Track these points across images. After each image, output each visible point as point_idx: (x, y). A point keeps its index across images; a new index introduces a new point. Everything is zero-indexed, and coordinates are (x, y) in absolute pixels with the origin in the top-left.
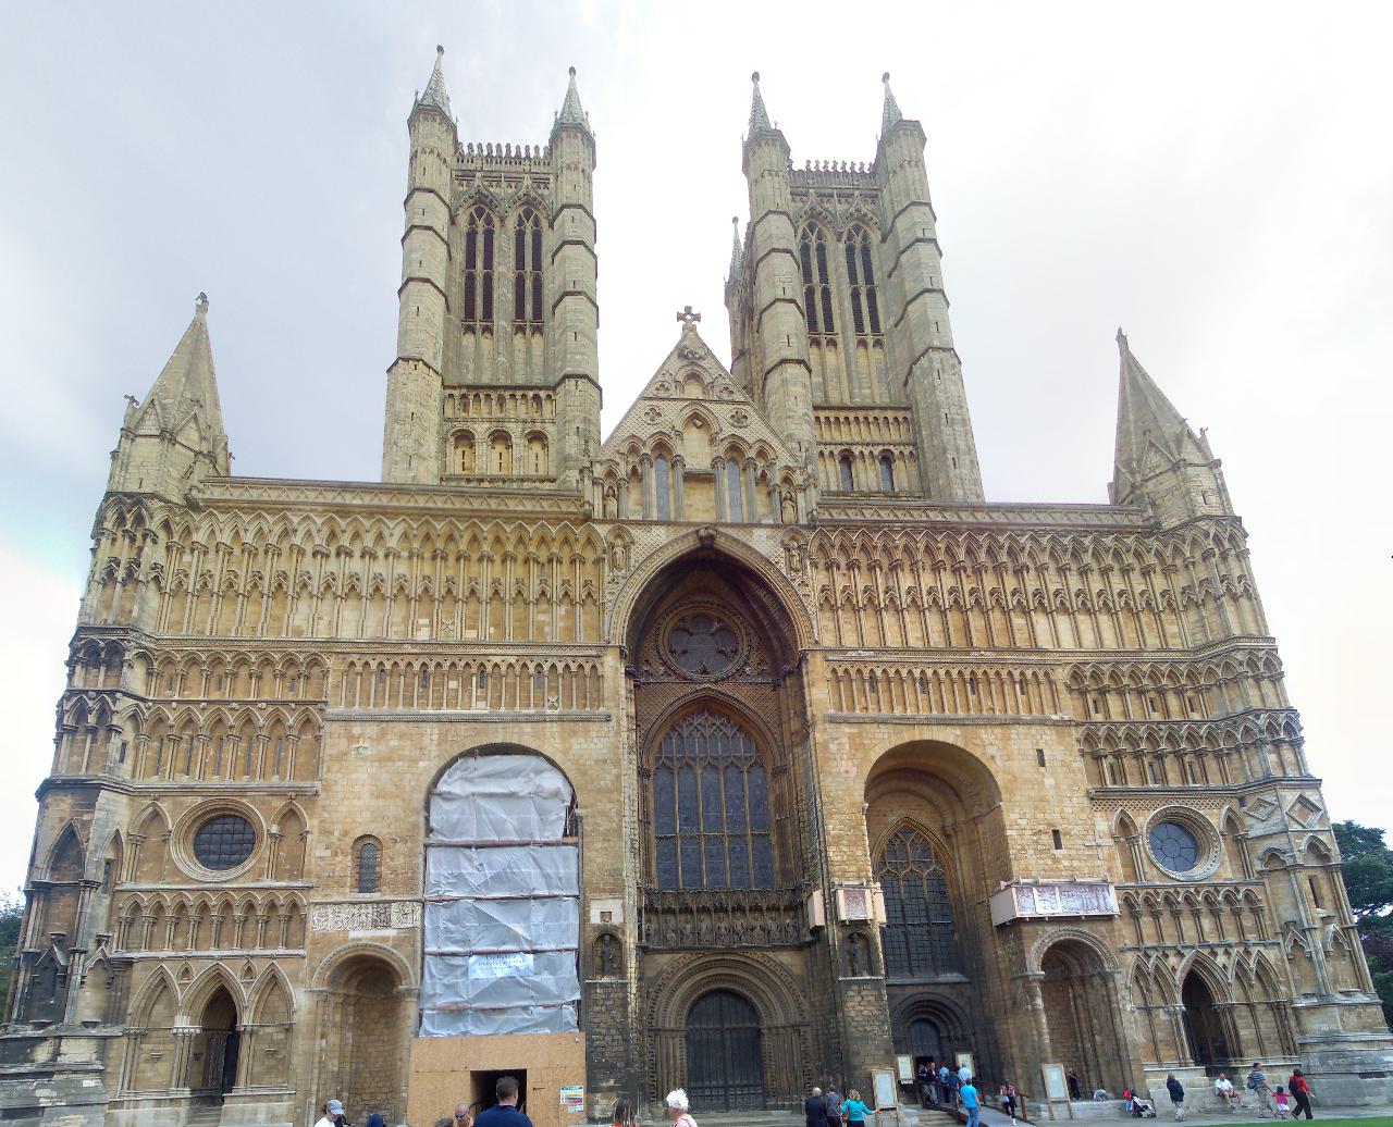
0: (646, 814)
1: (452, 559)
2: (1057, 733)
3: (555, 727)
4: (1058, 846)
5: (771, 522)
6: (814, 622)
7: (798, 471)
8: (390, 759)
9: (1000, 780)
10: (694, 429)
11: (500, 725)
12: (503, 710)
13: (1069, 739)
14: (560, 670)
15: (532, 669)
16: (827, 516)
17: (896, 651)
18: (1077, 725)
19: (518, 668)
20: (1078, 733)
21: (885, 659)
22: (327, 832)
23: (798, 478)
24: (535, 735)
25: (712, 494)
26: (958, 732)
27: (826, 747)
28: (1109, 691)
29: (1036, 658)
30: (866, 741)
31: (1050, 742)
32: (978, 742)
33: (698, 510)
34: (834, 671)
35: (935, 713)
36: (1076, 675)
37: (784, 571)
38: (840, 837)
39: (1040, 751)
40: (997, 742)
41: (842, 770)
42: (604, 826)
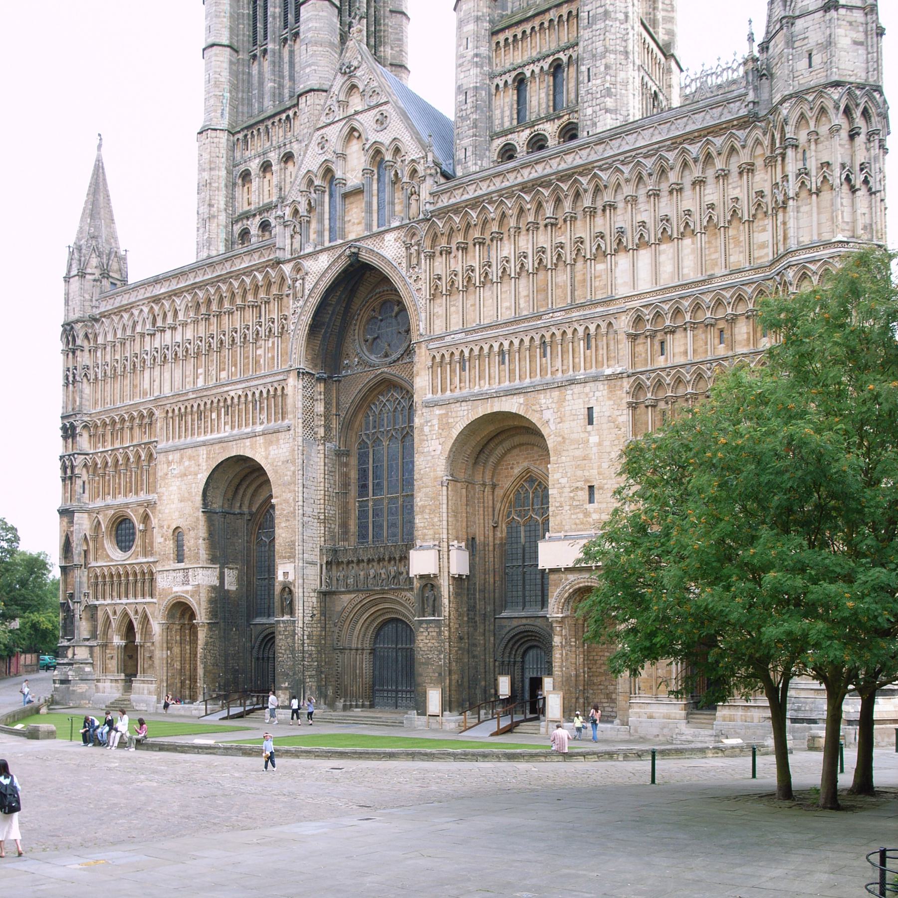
0: (346, 485)
1: (211, 317)
2: (609, 387)
3: (260, 440)
4: (591, 501)
5: (397, 224)
6: (423, 315)
7: (422, 161)
8: (185, 475)
9: (550, 443)
10: (355, 141)
11: (234, 443)
12: (236, 431)
13: (619, 392)
14: (265, 395)
15: (250, 398)
16: (440, 205)
17: (490, 327)
18: (628, 376)
19: (243, 399)
20: (626, 384)
21: (471, 339)
22: (161, 527)
23: (420, 168)
24: (252, 447)
25: (363, 205)
26: (521, 400)
27: (422, 430)
28: (673, 332)
29: (602, 309)
30: (451, 420)
31: (601, 399)
32: (537, 408)
33: (354, 224)
34: (434, 357)
35: (507, 383)
36: (638, 320)
37: (404, 273)
38: (424, 507)
39: (590, 409)
40: (554, 405)
41: (431, 449)
42: (288, 510)
